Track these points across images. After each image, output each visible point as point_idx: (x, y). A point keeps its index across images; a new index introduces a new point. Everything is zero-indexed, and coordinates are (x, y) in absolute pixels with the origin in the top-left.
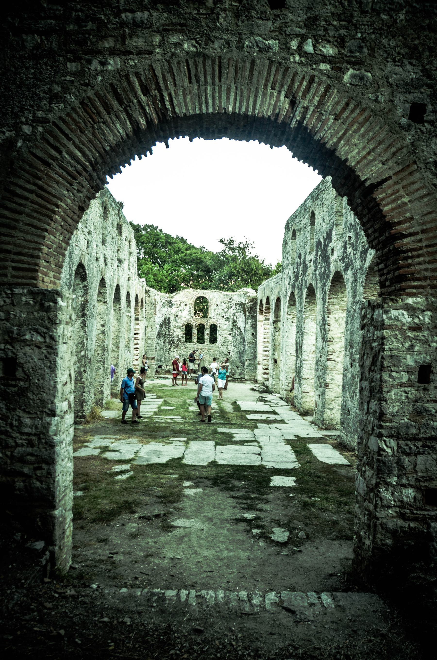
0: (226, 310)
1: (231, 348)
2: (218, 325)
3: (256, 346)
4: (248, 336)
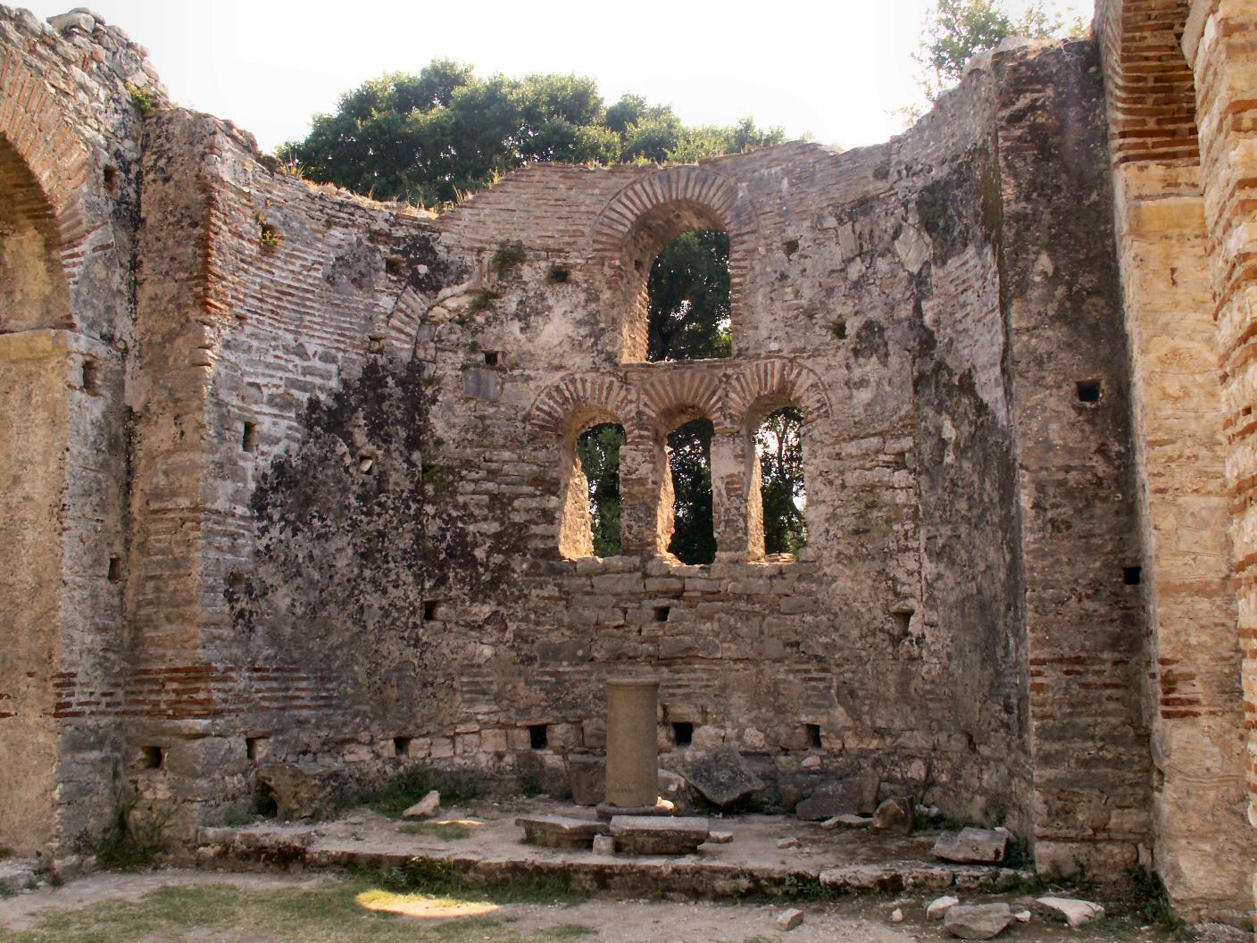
0: (856, 270)
1: (916, 569)
2: (810, 402)
3: (1129, 511)
4: (1043, 423)
